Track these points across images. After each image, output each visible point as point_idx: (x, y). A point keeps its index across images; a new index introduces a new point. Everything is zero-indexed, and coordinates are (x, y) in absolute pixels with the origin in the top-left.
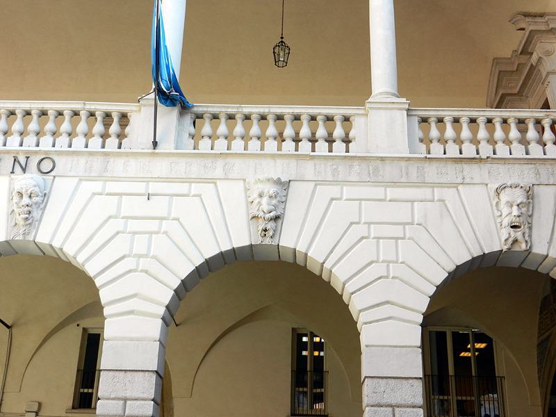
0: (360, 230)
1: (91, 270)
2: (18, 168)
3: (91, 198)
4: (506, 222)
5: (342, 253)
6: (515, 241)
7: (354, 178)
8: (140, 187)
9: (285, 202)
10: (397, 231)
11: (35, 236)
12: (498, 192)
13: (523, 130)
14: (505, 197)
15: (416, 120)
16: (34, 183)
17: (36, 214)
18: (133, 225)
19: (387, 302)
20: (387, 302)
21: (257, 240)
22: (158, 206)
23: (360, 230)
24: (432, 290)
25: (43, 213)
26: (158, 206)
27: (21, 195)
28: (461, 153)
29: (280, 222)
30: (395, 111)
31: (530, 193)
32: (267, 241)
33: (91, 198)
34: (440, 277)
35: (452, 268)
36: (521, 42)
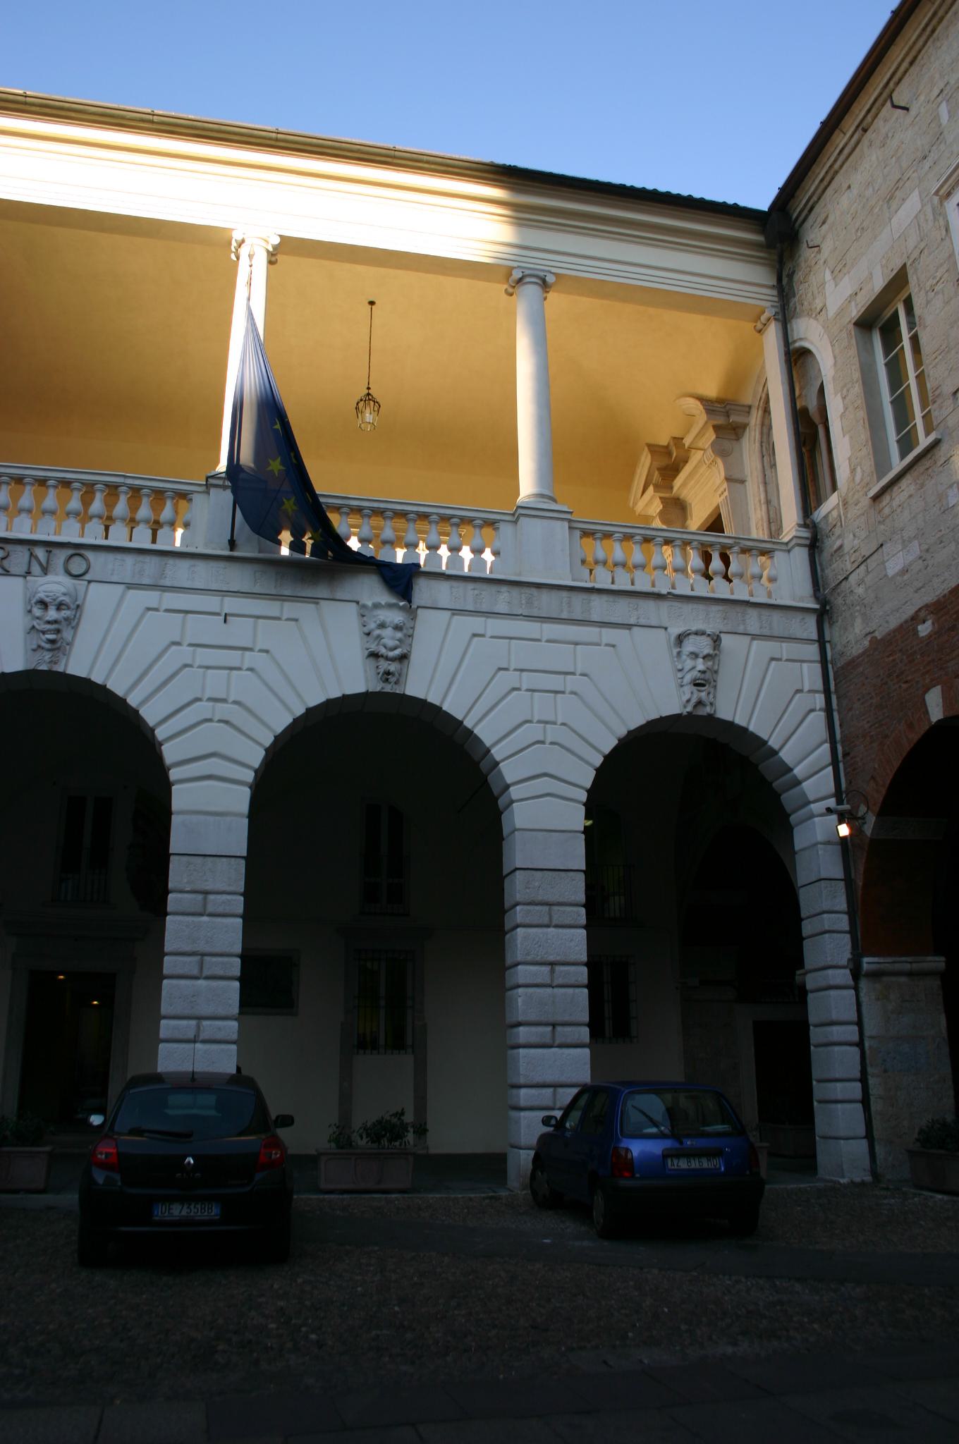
0: (510, 678)
1: (150, 715)
2: (36, 569)
3: (142, 616)
4: (688, 678)
5: (484, 711)
6: (700, 703)
7: (501, 608)
8: (212, 603)
9: (411, 636)
10: (555, 682)
11: (66, 666)
12: (680, 639)
13: (707, 558)
14: (690, 645)
15: (578, 533)
16: (63, 590)
17: (67, 634)
18: (204, 656)
19: (545, 775)
20: (545, 775)
21: (376, 686)
22: (239, 632)
23: (510, 678)
24: (598, 761)
25: (75, 634)
26: (239, 632)
27: (44, 604)
28: (633, 584)
29: (406, 662)
30: (559, 523)
31: (716, 640)
32: (388, 688)
33: (142, 616)
34: (609, 744)
35: (623, 732)
36: (918, 363)
